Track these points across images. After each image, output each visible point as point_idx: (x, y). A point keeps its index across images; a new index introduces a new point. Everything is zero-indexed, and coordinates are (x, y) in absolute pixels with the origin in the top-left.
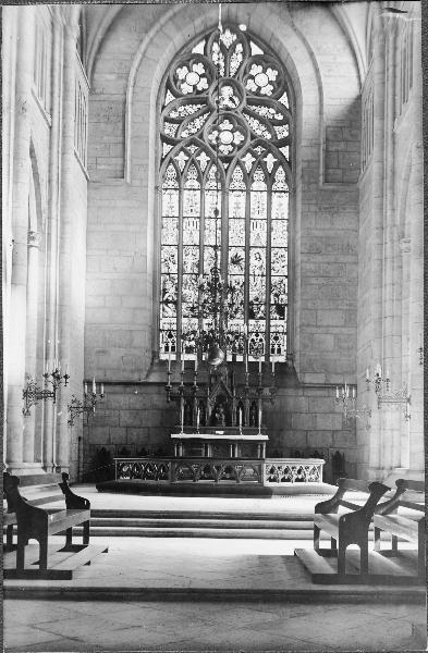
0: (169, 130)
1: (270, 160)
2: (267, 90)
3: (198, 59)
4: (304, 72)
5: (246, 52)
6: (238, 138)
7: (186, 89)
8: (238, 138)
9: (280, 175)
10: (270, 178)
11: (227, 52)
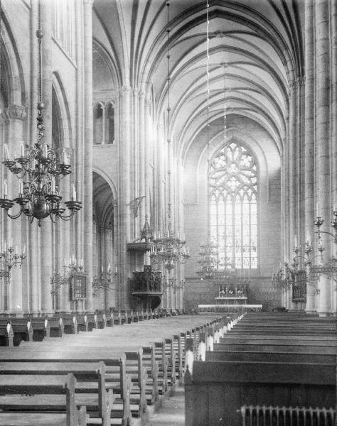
0: (212, 182)
1: (250, 191)
2: (248, 165)
3: (222, 154)
4: (260, 160)
5: (240, 151)
6: (238, 184)
7: (218, 166)
8: (238, 184)
9: (254, 197)
10: (250, 199)
11: (233, 151)
